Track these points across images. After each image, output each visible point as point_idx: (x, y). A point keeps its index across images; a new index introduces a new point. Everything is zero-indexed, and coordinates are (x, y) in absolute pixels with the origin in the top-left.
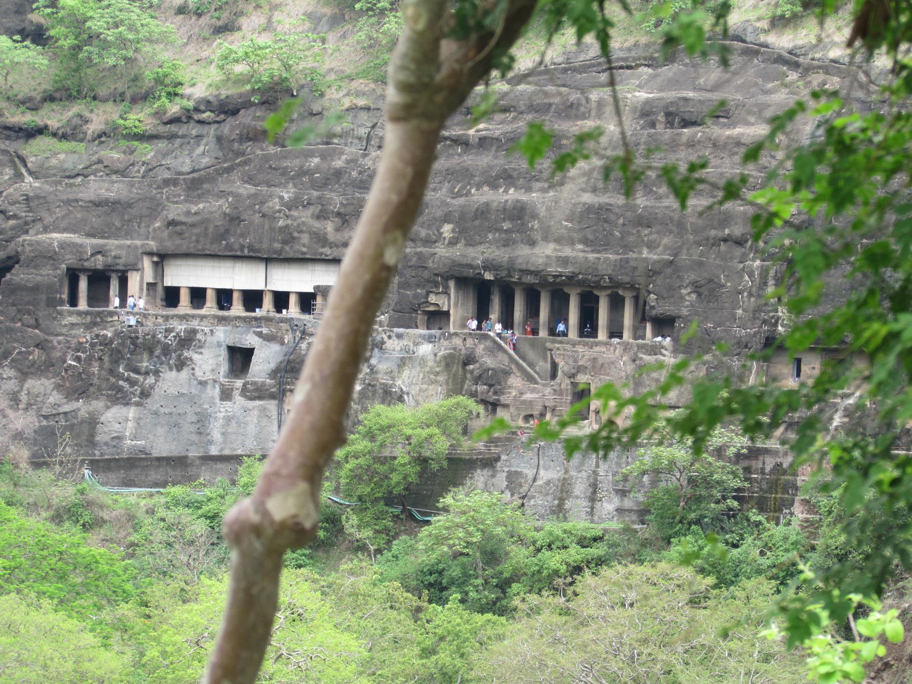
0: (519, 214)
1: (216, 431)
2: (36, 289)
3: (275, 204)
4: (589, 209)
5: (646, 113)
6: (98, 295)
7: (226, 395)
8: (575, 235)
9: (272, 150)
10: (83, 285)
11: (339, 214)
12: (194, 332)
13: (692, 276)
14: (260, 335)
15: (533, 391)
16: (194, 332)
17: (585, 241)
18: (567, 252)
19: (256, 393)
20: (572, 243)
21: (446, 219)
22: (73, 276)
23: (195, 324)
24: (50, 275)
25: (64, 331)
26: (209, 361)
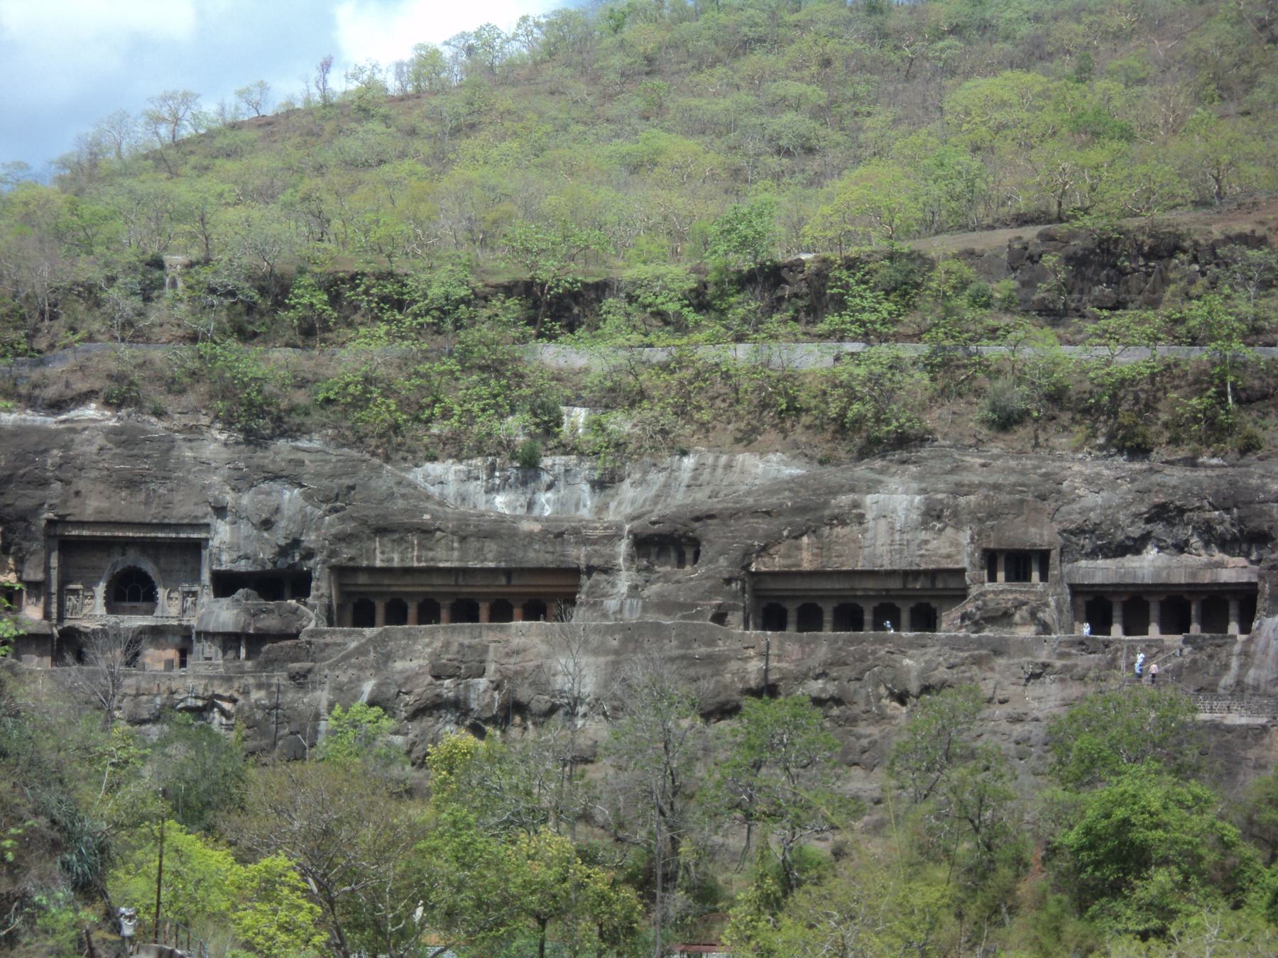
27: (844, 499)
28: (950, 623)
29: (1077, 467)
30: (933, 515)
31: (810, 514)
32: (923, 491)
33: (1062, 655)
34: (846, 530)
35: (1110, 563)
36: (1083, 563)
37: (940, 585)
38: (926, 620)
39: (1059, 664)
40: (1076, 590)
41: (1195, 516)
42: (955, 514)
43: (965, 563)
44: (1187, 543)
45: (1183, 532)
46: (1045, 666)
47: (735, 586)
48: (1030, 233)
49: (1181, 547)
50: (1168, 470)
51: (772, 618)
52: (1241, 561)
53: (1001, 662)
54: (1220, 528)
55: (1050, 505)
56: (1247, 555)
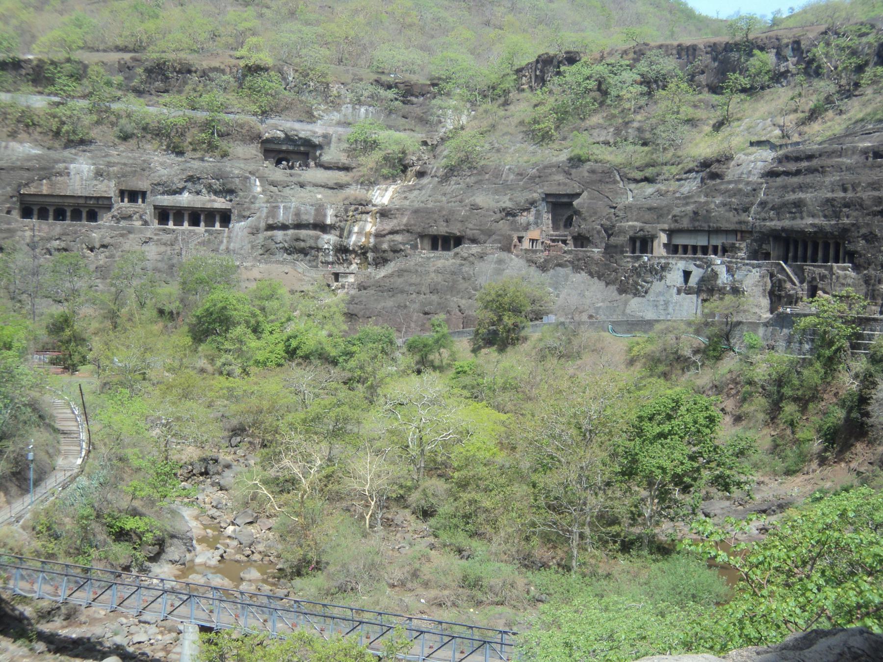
0: (799, 205)
1: (670, 310)
2: (616, 247)
3: (713, 206)
4: (828, 200)
5: (865, 152)
6: (644, 250)
7: (679, 292)
8: (821, 214)
9: (718, 181)
10: (638, 244)
11: (736, 209)
12: (669, 264)
13: (863, 231)
14: (695, 265)
15: (794, 289)
16: (669, 264)
17: (825, 216)
18: (816, 221)
19: (689, 291)
20: (819, 217)
21: (772, 209)
22: (633, 240)
23: (670, 261)
24: (622, 239)
25: (624, 264)
26: (675, 277)
27: (61, 166)
28: (106, 220)
29: (156, 158)
30: (99, 174)
31: (47, 171)
32: (94, 164)
33: (156, 234)
34: (62, 178)
35: (170, 197)
36: (159, 197)
37: (100, 202)
38: (93, 216)
39: (155, 238)
40: (156, 207)
41: (205, 181)
42: (108, 175)
43: (112, 195)
44: (200, 191)
45: (199, 187)
46: (150, 238)
47: (14, 199)
48: (127, 56)
49: (198, 193)
50: (193, 162)
51: (26, 213)
52: (223, 200)
53: (131, 236)
54: (215, 187)
55: (146, 173)
56: (225, 198)
